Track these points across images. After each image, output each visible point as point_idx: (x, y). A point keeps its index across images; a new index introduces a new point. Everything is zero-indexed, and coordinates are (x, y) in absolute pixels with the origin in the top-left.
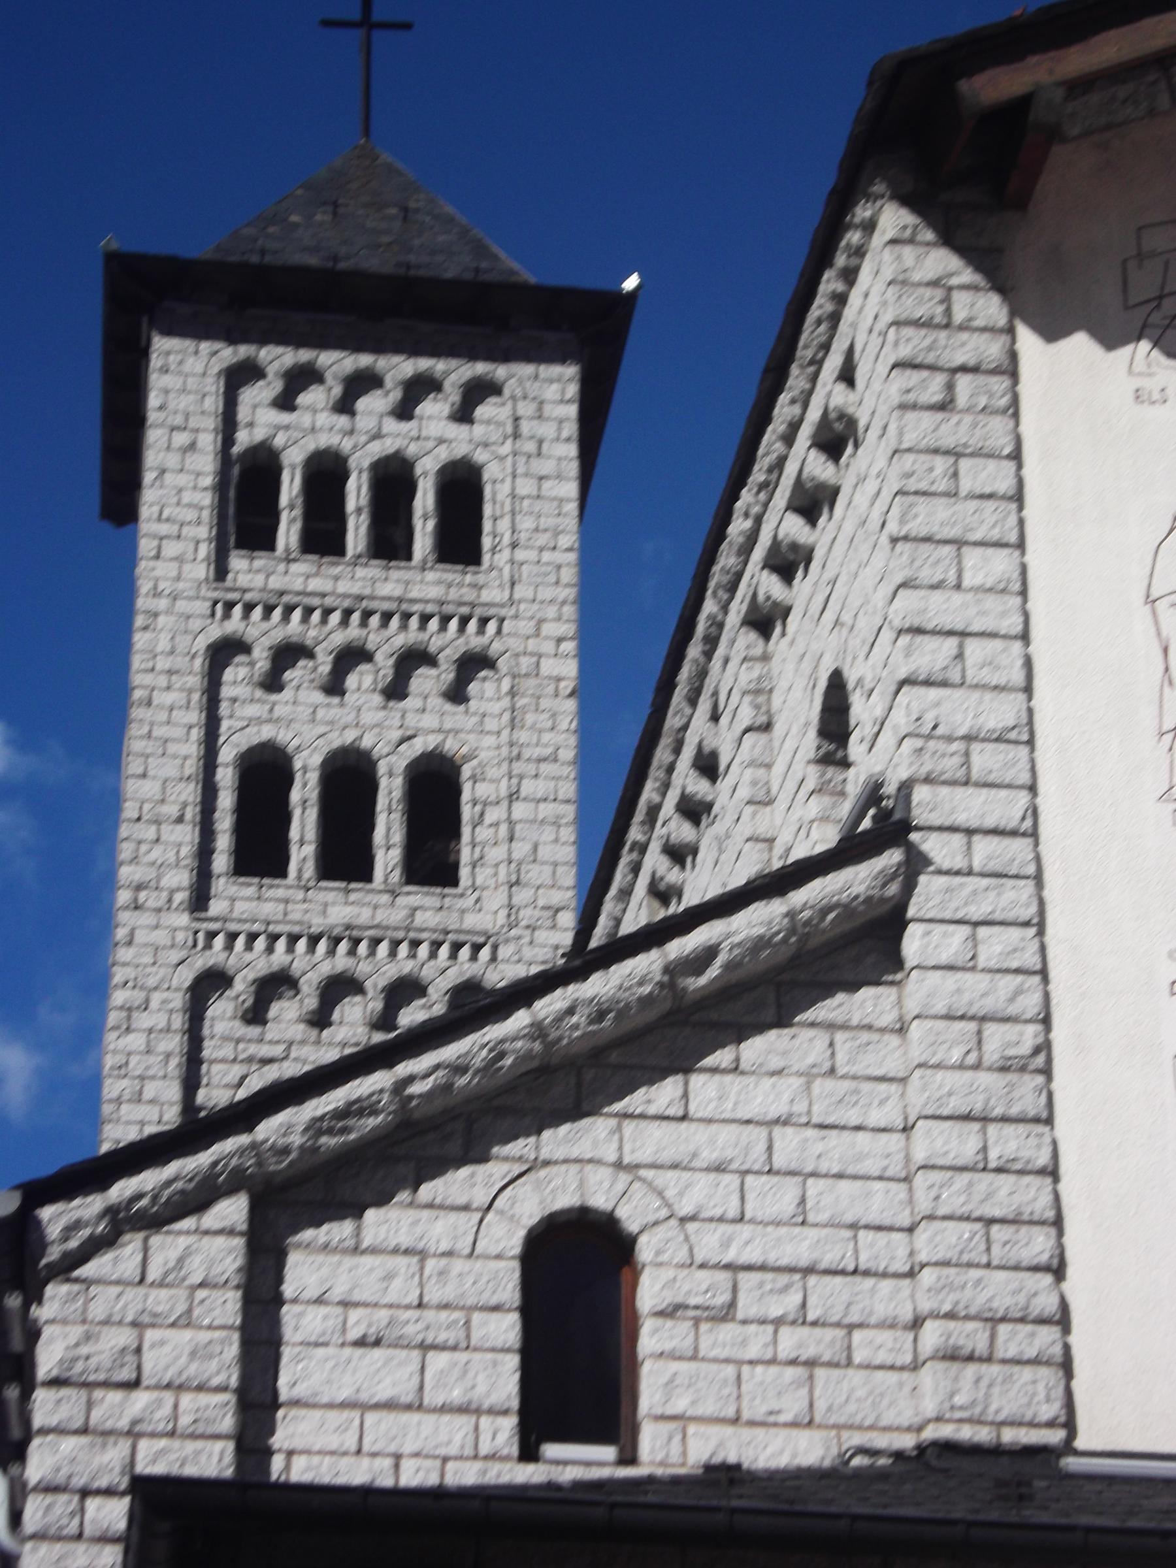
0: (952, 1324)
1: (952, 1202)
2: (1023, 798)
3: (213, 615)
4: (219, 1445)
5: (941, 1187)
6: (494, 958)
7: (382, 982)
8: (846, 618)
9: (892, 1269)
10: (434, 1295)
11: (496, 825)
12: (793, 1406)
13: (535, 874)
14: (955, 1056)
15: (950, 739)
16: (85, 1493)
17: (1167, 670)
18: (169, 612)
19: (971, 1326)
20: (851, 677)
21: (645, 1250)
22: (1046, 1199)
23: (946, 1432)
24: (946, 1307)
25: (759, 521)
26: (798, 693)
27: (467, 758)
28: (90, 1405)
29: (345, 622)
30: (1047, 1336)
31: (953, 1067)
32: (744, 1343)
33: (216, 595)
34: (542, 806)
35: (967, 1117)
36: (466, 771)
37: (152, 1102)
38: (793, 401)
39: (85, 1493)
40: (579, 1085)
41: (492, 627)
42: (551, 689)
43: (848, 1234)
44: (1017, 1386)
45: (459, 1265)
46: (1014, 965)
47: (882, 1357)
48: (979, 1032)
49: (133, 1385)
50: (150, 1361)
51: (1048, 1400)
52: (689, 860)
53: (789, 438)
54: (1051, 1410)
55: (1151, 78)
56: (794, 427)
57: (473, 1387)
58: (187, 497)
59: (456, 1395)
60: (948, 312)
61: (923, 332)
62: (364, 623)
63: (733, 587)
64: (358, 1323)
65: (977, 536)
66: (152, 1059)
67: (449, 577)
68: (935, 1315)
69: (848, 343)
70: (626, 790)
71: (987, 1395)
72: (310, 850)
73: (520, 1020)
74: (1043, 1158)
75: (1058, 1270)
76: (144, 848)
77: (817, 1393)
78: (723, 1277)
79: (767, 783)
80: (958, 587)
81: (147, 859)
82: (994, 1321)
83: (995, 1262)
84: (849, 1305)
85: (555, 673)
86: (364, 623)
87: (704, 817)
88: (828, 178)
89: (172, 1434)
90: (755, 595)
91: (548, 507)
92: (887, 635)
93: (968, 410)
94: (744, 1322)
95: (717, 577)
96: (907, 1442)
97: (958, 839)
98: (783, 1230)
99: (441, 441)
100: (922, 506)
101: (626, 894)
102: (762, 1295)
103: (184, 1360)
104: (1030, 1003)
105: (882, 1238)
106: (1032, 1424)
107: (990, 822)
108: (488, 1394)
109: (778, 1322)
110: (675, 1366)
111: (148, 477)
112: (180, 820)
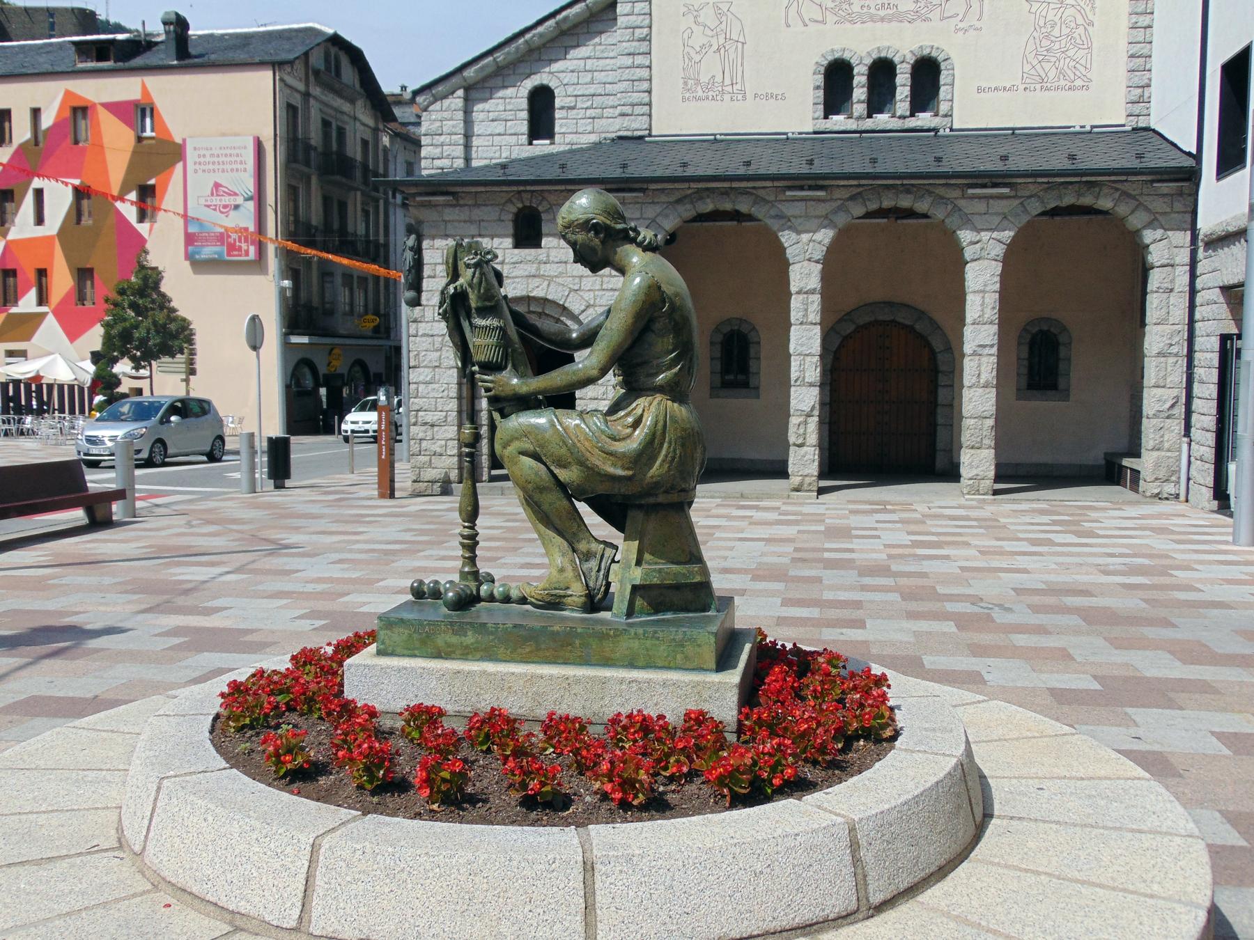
10: (508, 107)
12: (589, 128)
16: (433, 159)
21: (556, 92)
22: (648, 73)
30: (647, 108)
32: (578, 114)
35: (630, 54)
39: (433, 159)
45: (513, 101)
49: (441, 135)
54: (646, 126)
59: (512, 131)
64: (492, 116)
73: (521, 41)
74: (647, 63)
75: (650, 92)
78: (573, 99)
82: (633, 105)
96: (613, 135)
104: (647, 22)
109: (586, 108)
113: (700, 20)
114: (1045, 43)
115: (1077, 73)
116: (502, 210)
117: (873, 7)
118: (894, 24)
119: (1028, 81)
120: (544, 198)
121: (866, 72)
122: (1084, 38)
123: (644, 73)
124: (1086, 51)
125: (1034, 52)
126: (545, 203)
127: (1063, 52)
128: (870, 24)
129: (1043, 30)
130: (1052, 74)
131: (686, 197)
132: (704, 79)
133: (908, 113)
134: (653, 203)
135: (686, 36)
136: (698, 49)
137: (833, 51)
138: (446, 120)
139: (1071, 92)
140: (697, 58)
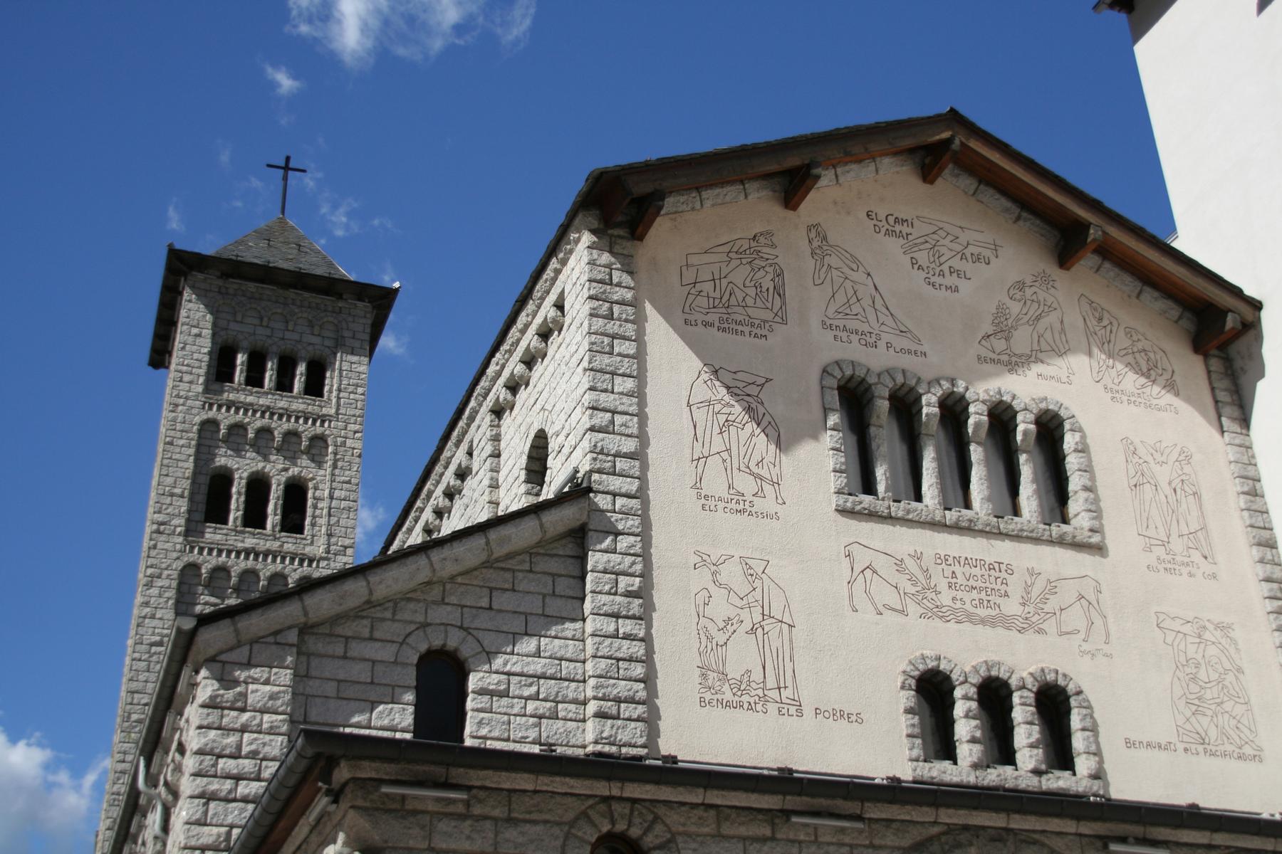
0: (602, 702)
1: (604, 651)
2: (637, 483)
3: (204, 408)
4: (280, 738)
5: (599, 644)
6: (318, 566)
7: (268, 574)
8: (548, 407)
9: (576, 678)
11: (322, 509)
12: (533, 734)
13: (336, 530)
14: (607, 588)
15: (608, 455)
17: (695, 434)
18: (183, 405)
19: (610, 703)
20: (550, 432)
23: (599, 748)
24: (600, 695)
25: (503, 367)
26: (516, 440)
27: (313, 479)
28: (222, 717)
29: (263, 416)
31: (606, 593)
33: (203, 399)
34: (343, 502)
36: (311, 485)
37: (160, 619)
38: (528, 315)
40: (444, 591)
41: (326, 424)
42: (350, 453)
43: (557, 662)
44: (628, 730)
46: (632, 552)
47: (570, 715)
48: (617, 580)
49: (243, 710)
50: (251, 699)
51: (641, 737)
52: (446, 515)
53: (523, 332)
55: (694, 195)
56: (527, 326)
57: (394, 720)
58: (196, 356)
60: (611, 278)
61: (601, 285)
62: (271, 417)
63: (485, 396)
65: (621, 371)
66: (162, 600)
67: (309, 401)
68: (595, 698)
69: (561, 289)
70: (417, 484)
71: (616, 733)
72: (240, 513)
76: (164, 507)
77: (542, 730)
78: (506, 677)
79: (497, 480)
80: (613, 392)
81: (166, 512)
82: (618, 700)
83: (620, 677)
84: (558, 692)
85: (353, 446)
86: (271, 417)
87: (457, 496)
88: (561, 218)
89: (260, 732)
90: (498, 397)
91: (354, 375)
92: (579, 410)
93: (619, 319)
94: (513, 698)
95: (478, 390)
97: (609, 497)
98: (530, 659)
99: (310, 344)
100: (598, 357)
101: (410, 531)
102: (521, 687)
103: (266, 699)
104: (638, 568)
105: (572, 665)
106: (634, 746)
107: (623, 490)
108: (400, 723)
109: (527, 699)
110: (482, 715)
111: (177, 345)
112: (182, 496)
113: (722, 578)
114: (1194, 688)
115: (1242, 735)
116: (567, 837)
117: (968, 602)
118: (1000, 631)
119: (1186, 739)
120: (656, 818)
121: (975, 696)
122: (1237, 689)
123: (638, 649)
124: (1244, 707)
125: (1183, 700)
126: (659, 828)
127: (1218, 704)
128: (967, 627)
129: (1188, 670)
130: (1213, 733)
131: (930, 839)
132: (734, 672)
133: (1043, 767)
134: (872, 846)
135: (700, 601)
136: (722, 625)
137: (923, 657)
138: (255, 681)
139: (1241, 764)
140: (721, 638)
